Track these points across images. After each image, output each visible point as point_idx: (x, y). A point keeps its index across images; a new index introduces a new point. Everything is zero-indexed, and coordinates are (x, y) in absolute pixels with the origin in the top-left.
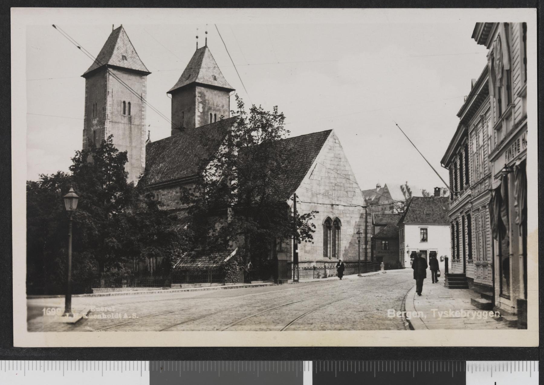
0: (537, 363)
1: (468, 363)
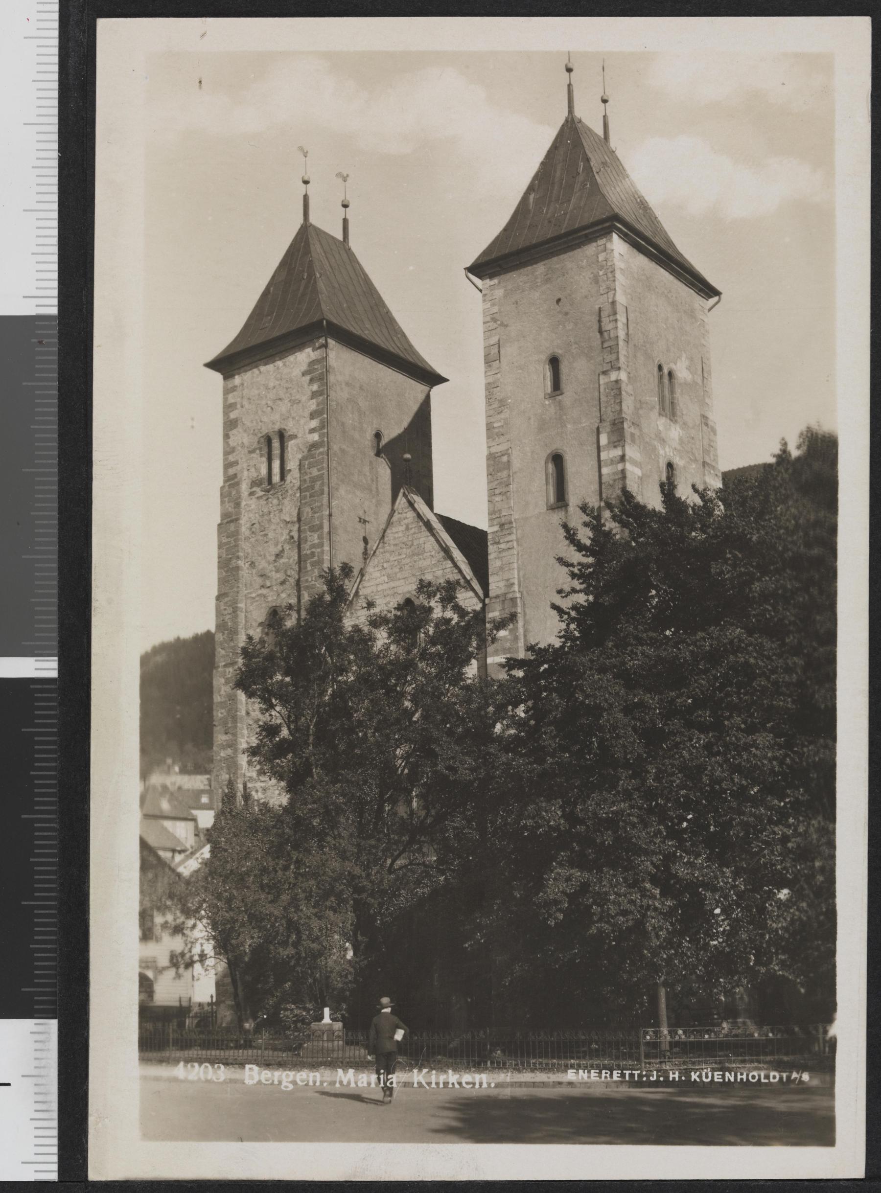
0: (54, 1177)
1: (53, 1025)
